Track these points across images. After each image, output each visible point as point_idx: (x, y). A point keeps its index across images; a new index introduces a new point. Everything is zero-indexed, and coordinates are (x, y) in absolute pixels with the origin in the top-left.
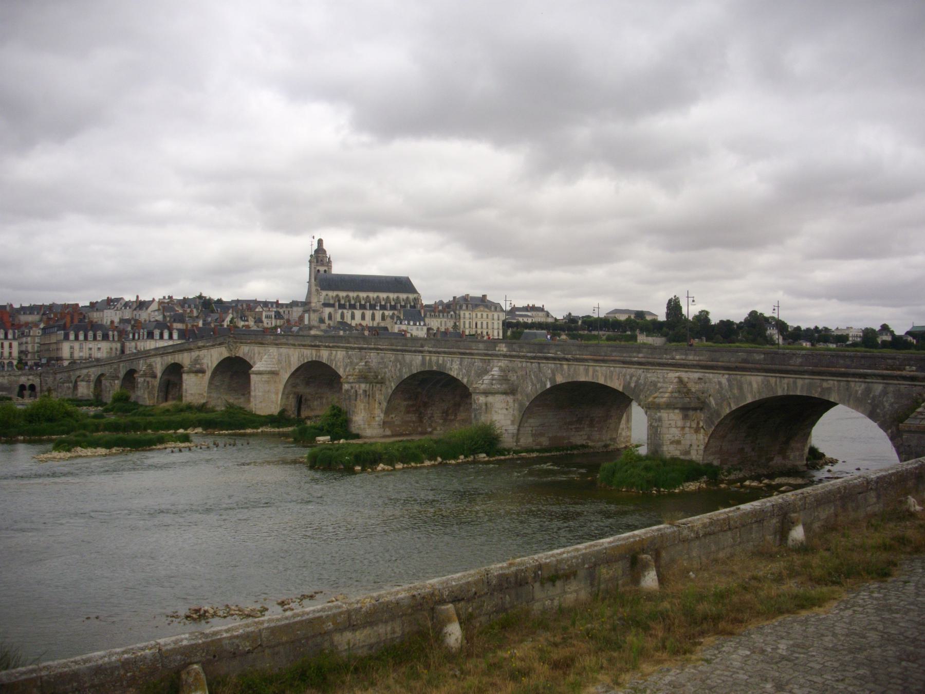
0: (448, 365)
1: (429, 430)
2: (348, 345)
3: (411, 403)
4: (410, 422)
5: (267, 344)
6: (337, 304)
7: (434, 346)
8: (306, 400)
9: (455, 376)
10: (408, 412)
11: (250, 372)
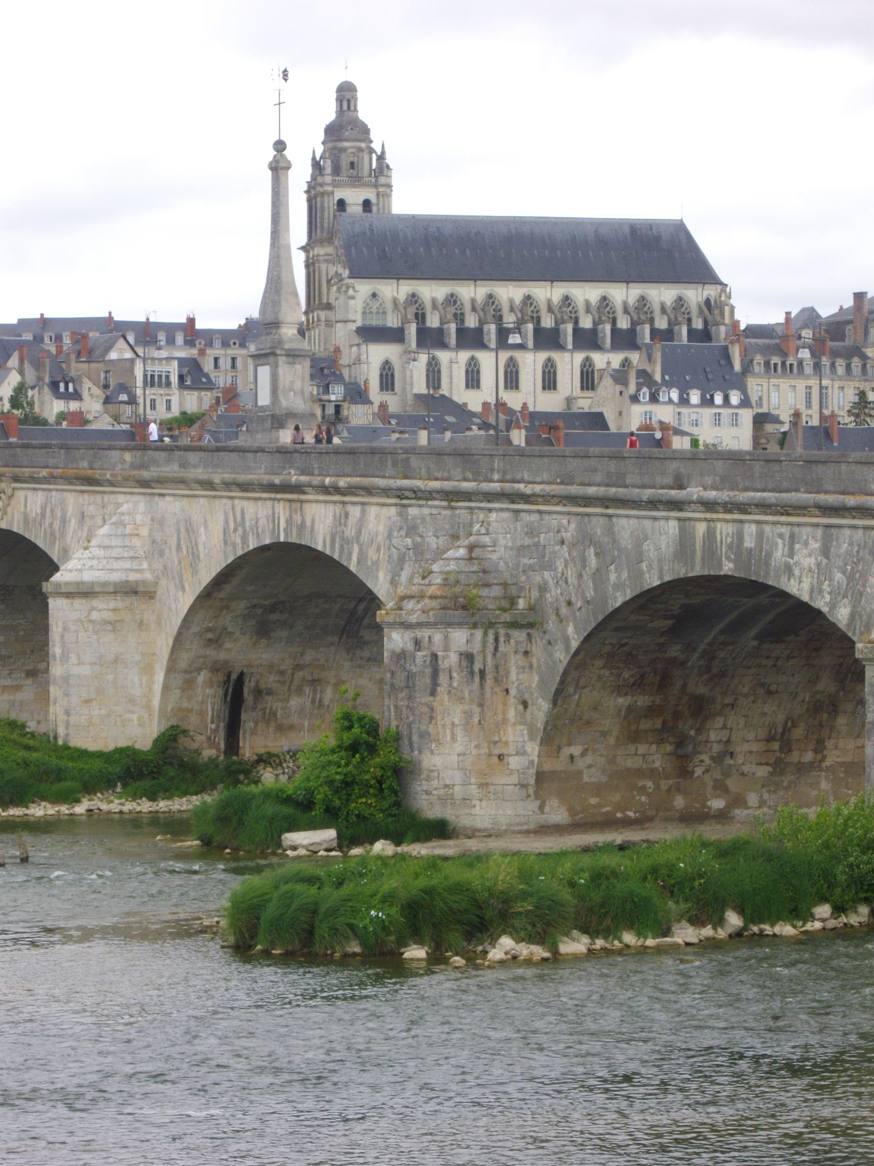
0: (779, 554)
1: (717, 804)
2: (406, 483)
3: (643, 701)
4: (640, 773)
5: (112, 484)
6: (412, 330)
7: (726, 482)
8: (258, 693)
9: (805, 598)
10: (635, 737)
11: (47, 587)
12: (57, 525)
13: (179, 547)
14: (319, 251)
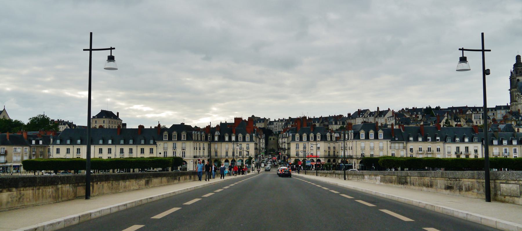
14: (513, 90)
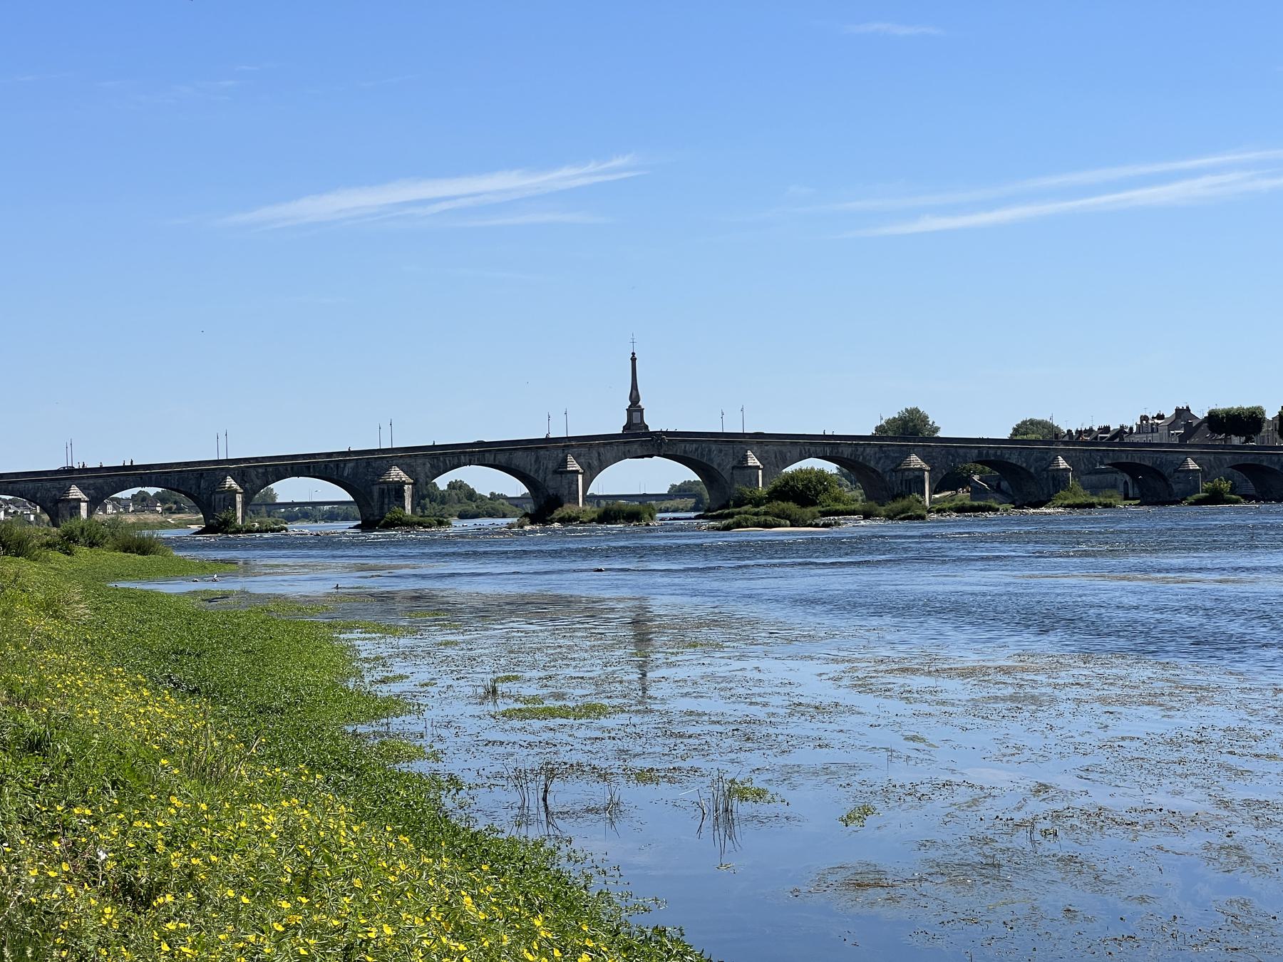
12: (705, 453)
13: (776, 457)
